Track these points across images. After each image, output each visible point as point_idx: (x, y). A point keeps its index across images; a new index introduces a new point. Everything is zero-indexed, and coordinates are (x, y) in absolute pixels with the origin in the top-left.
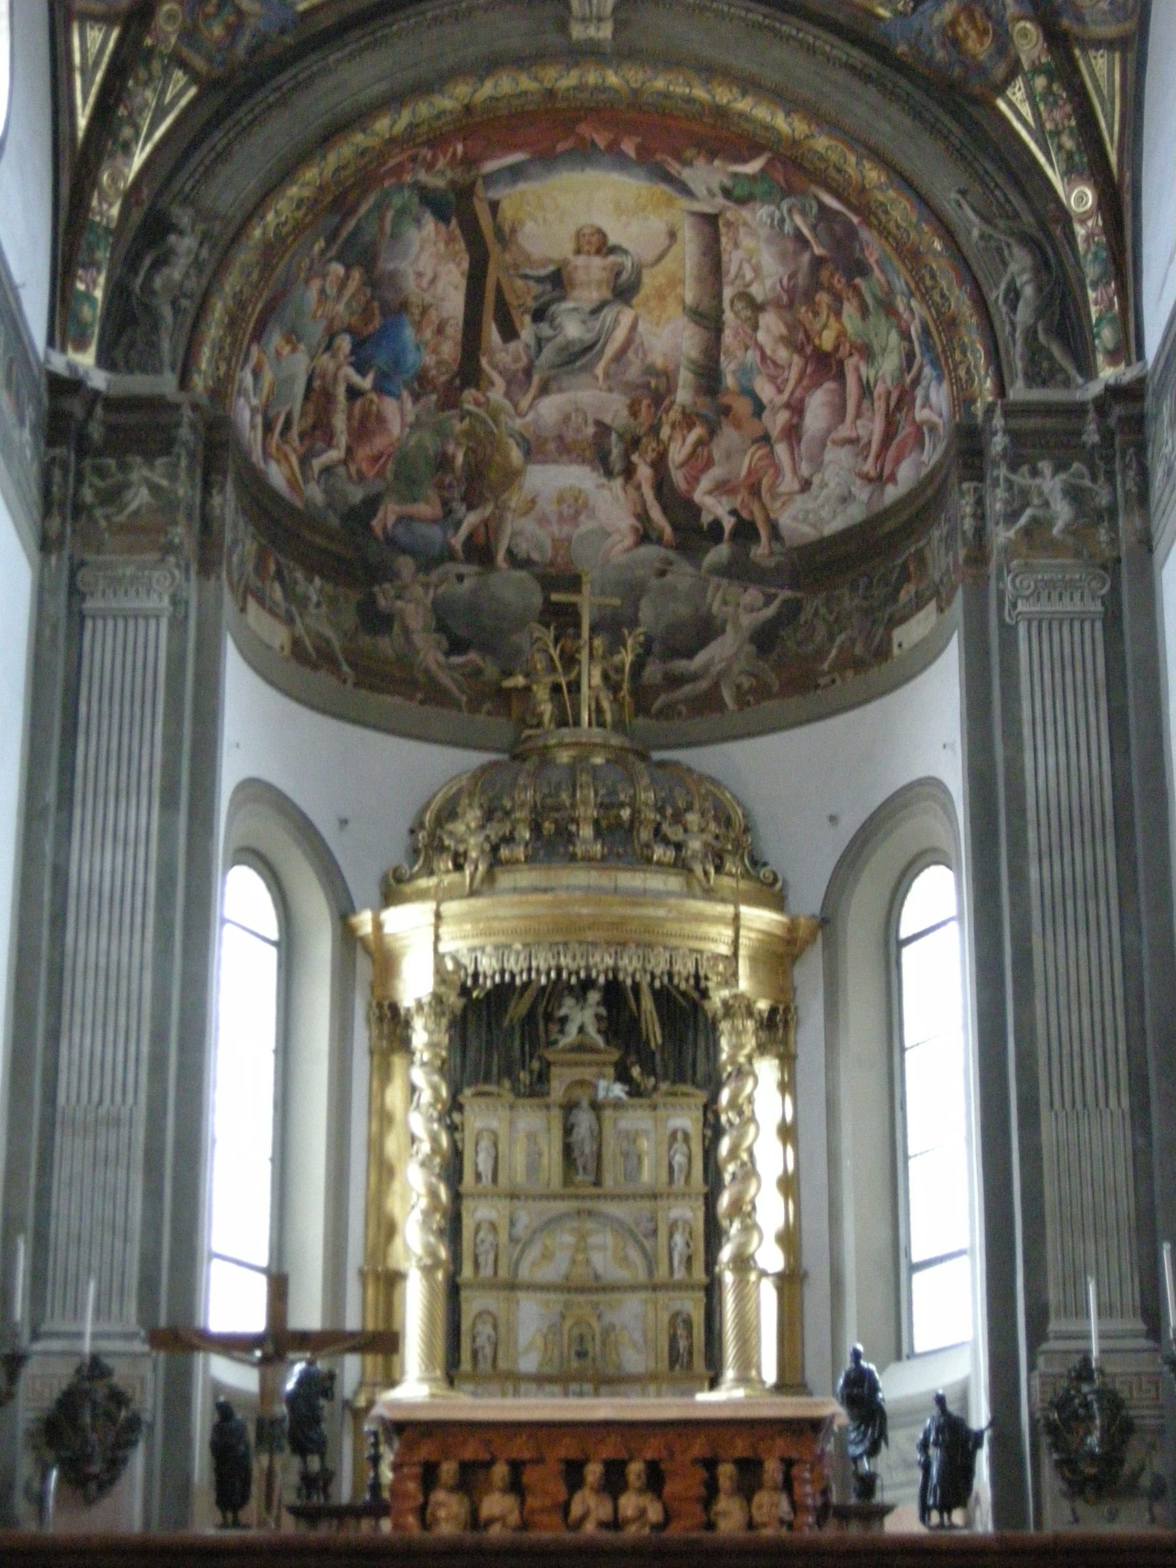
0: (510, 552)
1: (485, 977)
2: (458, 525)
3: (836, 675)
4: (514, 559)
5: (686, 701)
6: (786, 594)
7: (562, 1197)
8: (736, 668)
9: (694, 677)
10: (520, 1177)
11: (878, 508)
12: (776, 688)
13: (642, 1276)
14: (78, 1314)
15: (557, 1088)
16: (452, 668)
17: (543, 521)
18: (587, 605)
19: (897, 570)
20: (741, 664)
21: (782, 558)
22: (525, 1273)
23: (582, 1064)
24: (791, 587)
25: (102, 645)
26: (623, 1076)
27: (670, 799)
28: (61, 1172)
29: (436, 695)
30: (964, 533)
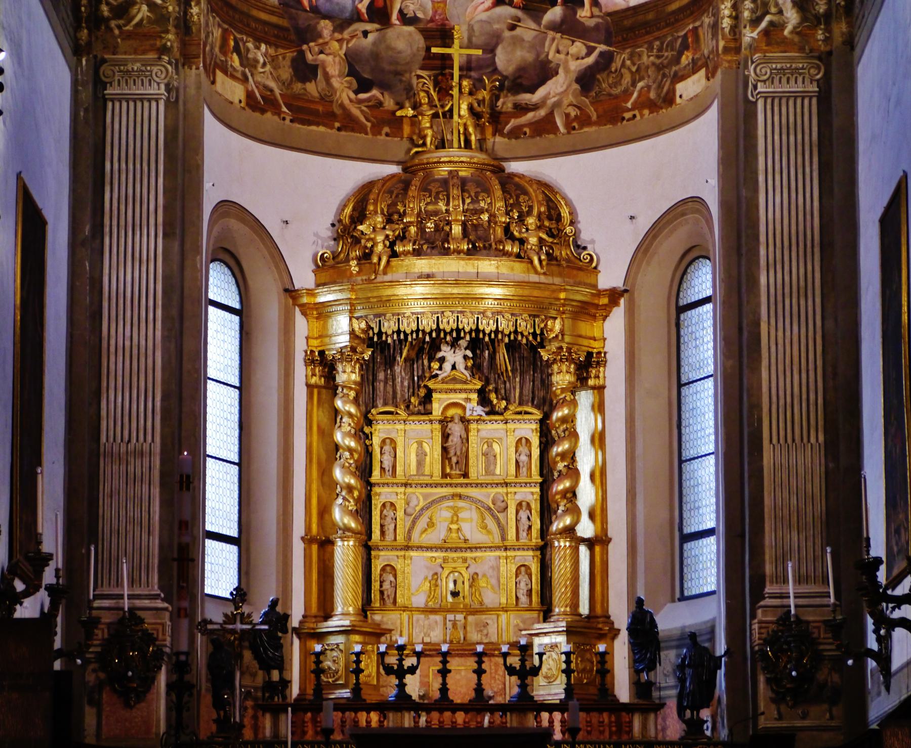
0: (401, 11)
1: (387, 336)
3: (636, 112)
6: (602, 48)
7: (441, 485)
9: (535, 107)
10: (413, 470)
12: (594, 117)
13: (497, 541)
14: (119, 584)
15: (437, 408)
16: (360, 102)
18: (457, 53)
20: (571, 98)
21: (600, 20)
22: (416, 538)
23: (455, 391)
24: (605, 44)
25: (119, 120)
26: (484, 400)
27: (517, 204)
28: (105, 488)
29: (349, 124)
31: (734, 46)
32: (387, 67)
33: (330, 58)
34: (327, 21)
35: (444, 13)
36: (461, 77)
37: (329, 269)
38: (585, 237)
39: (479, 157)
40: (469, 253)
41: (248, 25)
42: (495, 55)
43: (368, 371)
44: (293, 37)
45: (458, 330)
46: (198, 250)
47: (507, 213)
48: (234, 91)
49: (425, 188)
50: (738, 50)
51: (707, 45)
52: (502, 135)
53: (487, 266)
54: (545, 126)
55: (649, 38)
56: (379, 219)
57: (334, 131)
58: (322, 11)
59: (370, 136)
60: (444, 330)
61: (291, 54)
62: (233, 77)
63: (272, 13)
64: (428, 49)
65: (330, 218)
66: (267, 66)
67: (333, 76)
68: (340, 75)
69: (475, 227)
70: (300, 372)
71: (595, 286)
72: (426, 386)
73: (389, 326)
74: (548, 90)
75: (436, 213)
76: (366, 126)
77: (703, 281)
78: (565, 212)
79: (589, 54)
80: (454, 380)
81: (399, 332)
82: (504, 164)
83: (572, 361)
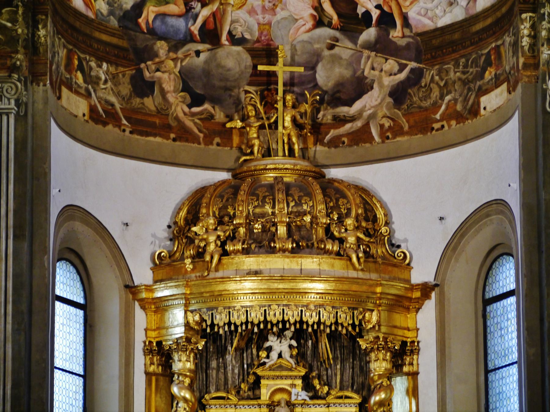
0: (230, 33)
1: (219, 328)
2: (196, 17)
3: (445, 123)
4: (234, 40)
5: (348, 135)
6: (413, 65)
8: (380, 114)
9: (352, 119)
11: (473, 12)
15: (265, 394)
16: (193, 115)
17: (252, 12)
18: (281, 70)
19: (483, 58)
20: (385, 110)
21: (411, 40)
23: (281, 377)
26: (308, 386)
27: (337, 207)
29: (184, 135)
30: (523, 47)
31: (533, 63)
32: (217, 83)
33: (166, 76)
34: (163, 42)
35: (269, 34)
36: (285, 92)
37: (166, 266)
38: (399, 236)
39: (302, 164)
40: (293, 251)
41: (91, 46)
42: (315, 72)
43: (201, 360)
44: (132, 56)
45: (284, 322)
46: (45, 251)
47: (328, 215)
48: (79, 106)
49: (252, 193)
50: (536, 66)
51: (508, 61)
52: (323, 144)
53: (310, 263)
54: (361, 136)
55: (455, 56)
56: (211, 221)
57: (170, 141)
58: (159, 33)
59: (202, 146)
60: (271, 322)
61: (130, 72)
62: (77, 93)
63: (113, 35)
64: (255, 67)
65: (167, 220)
66: (109, 84)
67: (168, 92)
68: (174, 91)
69: (299, 228)
70: (140, 361)
71: (408, 281)
72: (255, 374)
73: (221, 319)
74: (364, 103)
75: (263, 215)
76: (199, 137)
77: (507, 277)
78: (380, 214)
79: (400, 71)
80: (281, 367)
81: (229, 324)
82: (325, 171)
83: (388, 349)
